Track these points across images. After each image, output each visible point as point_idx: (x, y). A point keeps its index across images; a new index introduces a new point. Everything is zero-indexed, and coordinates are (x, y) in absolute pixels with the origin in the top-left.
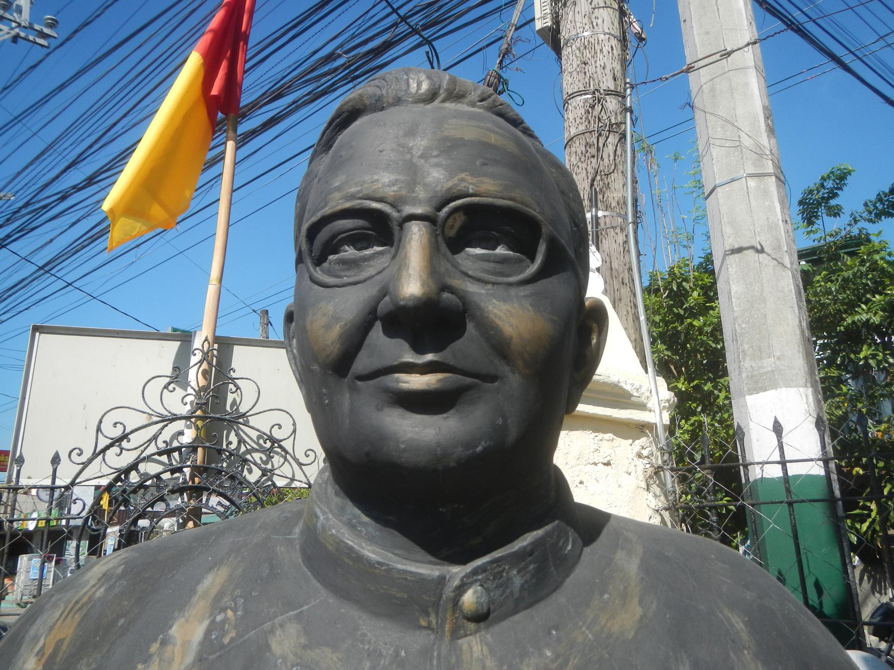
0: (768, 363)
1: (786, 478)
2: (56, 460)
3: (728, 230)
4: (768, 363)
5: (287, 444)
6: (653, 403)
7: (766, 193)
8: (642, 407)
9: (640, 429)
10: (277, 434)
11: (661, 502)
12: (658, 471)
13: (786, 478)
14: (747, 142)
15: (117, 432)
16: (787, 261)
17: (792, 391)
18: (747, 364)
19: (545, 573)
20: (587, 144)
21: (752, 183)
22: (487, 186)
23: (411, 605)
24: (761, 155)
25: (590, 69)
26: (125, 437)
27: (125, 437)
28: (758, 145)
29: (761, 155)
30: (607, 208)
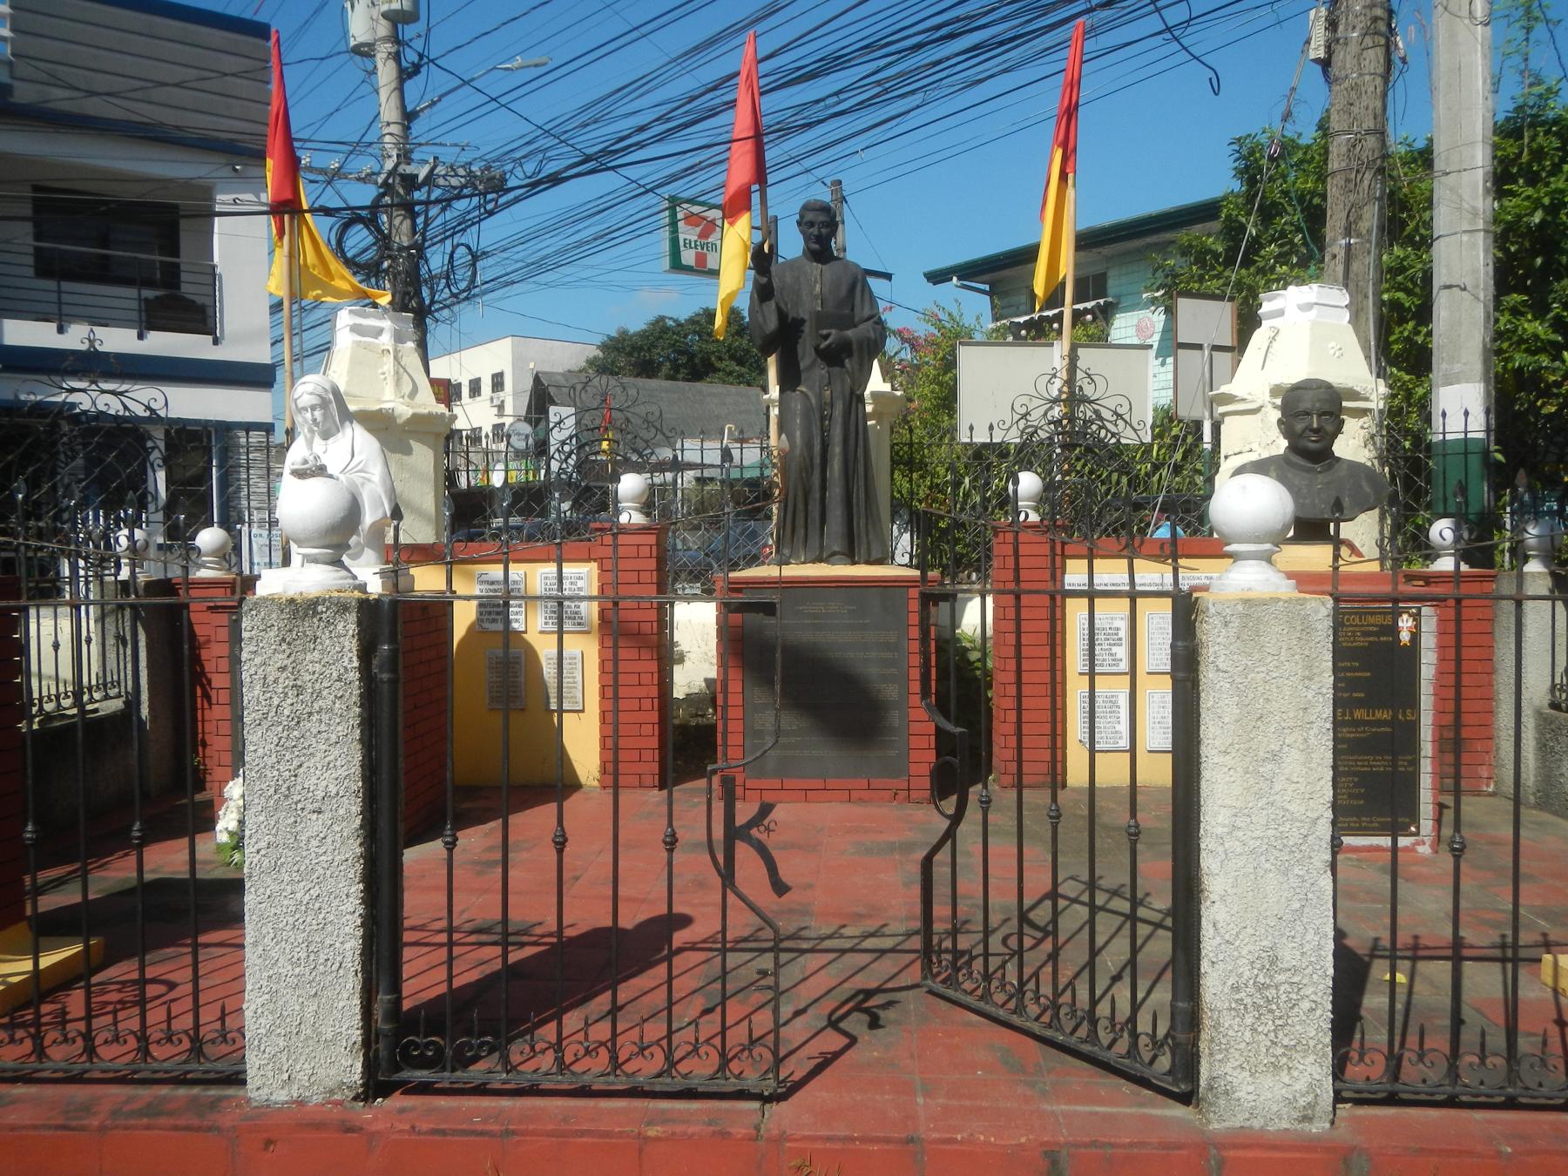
0: (1457, 367)
1: (1466, 439)
2: (991, 428)
3: (1444, 271)
4: (1457, 367)
5: (1127, 417)
6: (1374, 397)
7: (1474, 246)
8: (1367, 399)
9: (1364, 412)
10: (1120, 411)
11: (1374, 454)
12: (1373, 437)
13: (1466, 439)
14: (1466, 206)
15: (1023, 410)
16: (1482, 296)
17: (1470, 385)
18: (1444, 366)
19: (1330, 467)
20: (1348, 180)
21: (1465, 238)
22: (1326, 408)
23: (1308, 470)
24: (1475, 215)
25: (1355, 110)
26: (1028, 413)
27: (1028, 413)
28: (1474, 208)
29: (1475, 215)
30: (1359, 235)
